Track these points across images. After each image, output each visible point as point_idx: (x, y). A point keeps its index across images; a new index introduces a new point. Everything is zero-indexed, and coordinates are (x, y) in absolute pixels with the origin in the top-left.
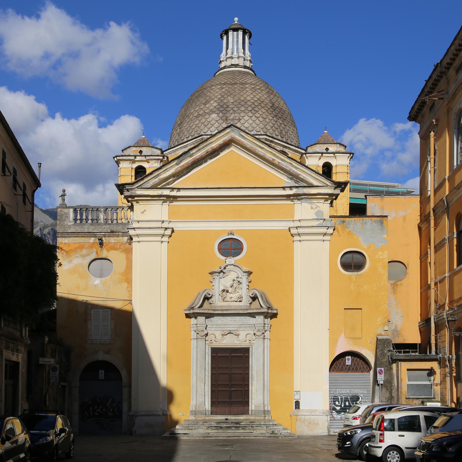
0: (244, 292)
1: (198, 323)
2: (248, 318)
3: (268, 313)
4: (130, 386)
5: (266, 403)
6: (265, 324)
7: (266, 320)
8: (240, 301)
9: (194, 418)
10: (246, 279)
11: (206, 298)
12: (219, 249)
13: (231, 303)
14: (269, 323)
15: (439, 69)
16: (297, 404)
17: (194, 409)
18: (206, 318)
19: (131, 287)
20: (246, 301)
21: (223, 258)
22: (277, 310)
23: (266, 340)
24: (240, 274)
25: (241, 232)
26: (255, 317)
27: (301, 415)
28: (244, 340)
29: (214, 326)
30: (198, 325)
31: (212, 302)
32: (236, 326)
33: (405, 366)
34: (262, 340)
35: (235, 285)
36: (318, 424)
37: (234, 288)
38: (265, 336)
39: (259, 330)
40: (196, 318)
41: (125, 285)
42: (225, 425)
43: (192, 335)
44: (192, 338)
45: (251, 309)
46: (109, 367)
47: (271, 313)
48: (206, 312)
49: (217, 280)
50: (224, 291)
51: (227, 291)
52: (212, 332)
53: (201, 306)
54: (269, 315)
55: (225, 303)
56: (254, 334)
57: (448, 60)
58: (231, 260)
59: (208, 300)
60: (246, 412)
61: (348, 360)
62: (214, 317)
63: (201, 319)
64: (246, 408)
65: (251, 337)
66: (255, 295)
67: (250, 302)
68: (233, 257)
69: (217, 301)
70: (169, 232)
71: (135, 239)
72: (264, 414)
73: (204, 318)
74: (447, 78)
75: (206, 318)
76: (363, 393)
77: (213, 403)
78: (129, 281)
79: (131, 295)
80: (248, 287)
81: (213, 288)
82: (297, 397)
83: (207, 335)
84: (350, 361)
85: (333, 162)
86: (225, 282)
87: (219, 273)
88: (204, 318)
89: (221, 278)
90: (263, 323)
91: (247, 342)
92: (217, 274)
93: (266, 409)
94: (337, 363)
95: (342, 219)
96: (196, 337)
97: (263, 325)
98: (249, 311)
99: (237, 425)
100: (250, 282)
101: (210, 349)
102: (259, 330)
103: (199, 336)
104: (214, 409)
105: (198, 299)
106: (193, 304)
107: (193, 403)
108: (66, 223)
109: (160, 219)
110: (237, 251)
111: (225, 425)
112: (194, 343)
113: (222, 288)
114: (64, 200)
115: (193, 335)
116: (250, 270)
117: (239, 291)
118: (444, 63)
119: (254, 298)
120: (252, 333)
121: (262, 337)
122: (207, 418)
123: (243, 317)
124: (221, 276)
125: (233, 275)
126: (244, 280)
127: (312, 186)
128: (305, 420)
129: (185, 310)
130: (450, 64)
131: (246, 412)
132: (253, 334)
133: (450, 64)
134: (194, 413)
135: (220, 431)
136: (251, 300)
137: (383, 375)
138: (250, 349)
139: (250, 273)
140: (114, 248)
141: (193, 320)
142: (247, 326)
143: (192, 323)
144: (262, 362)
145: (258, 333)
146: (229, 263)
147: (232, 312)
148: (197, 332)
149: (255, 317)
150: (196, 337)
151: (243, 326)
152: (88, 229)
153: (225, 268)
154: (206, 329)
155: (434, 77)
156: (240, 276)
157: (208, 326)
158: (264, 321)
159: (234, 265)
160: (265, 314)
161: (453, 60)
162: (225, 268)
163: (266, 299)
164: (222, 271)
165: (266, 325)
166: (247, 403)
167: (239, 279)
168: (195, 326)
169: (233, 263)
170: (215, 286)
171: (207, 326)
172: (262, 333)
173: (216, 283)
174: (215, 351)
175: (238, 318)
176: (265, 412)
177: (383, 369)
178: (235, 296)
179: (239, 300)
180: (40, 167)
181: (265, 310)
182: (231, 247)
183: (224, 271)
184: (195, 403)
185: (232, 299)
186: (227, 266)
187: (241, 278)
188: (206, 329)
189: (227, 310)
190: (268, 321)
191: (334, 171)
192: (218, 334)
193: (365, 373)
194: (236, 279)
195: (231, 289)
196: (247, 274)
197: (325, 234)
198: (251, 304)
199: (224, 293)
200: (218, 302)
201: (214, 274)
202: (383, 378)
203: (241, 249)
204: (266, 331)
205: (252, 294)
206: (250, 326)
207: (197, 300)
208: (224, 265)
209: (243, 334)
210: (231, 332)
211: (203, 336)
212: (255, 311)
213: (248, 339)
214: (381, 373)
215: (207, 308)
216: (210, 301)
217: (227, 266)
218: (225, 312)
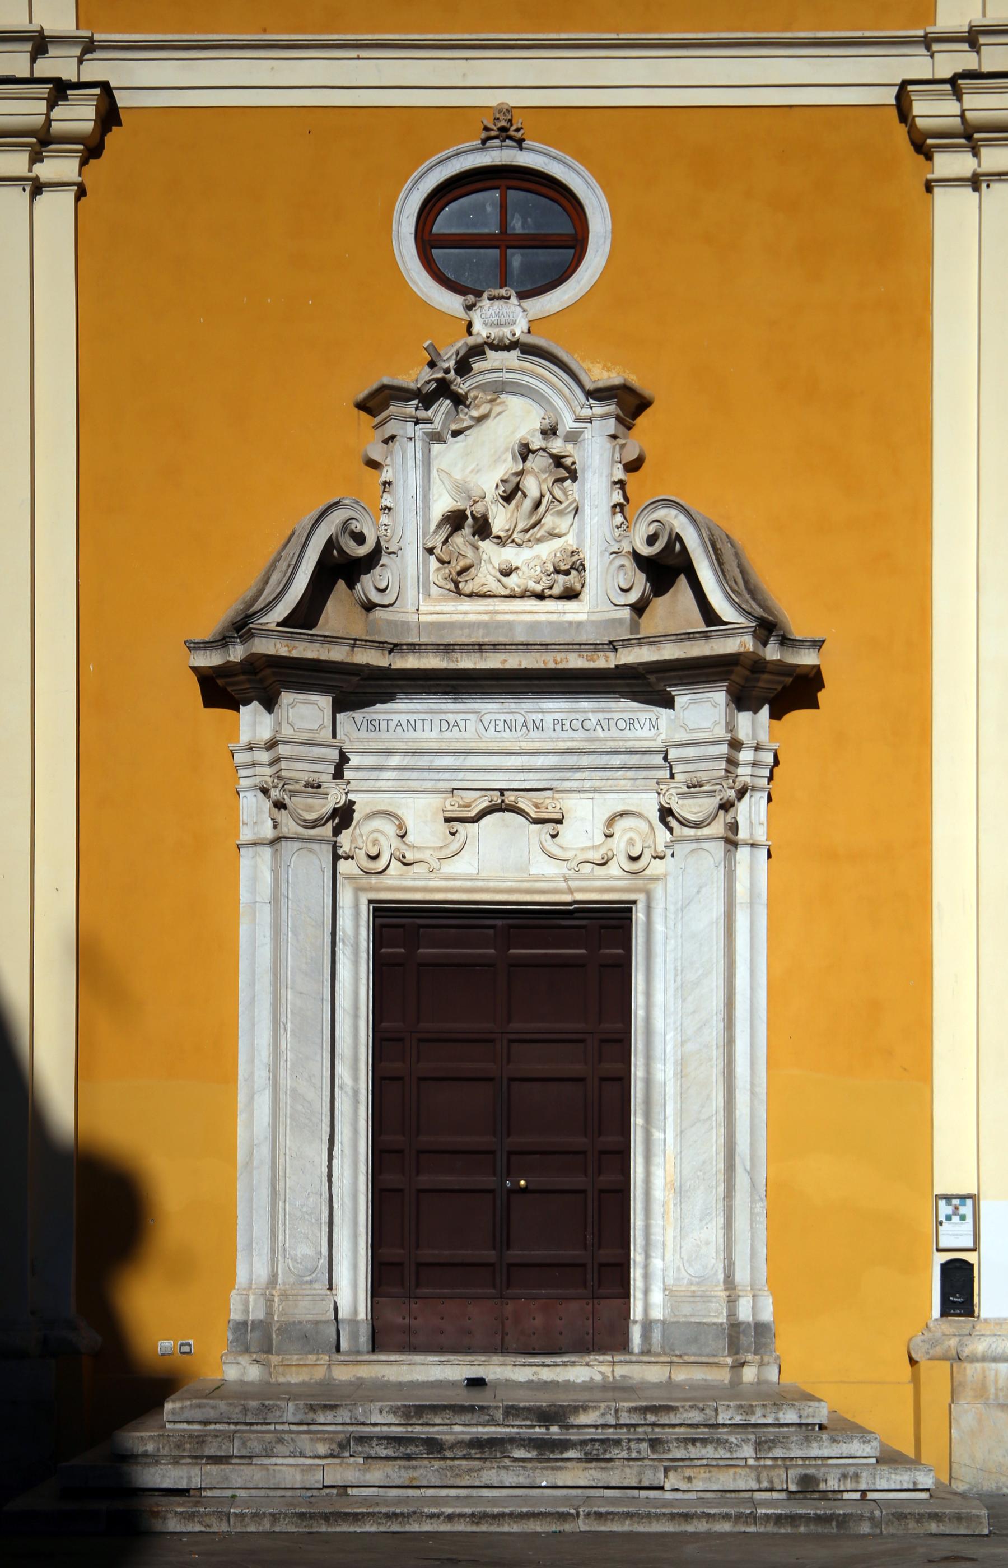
0: (594, 530)
1: (287, 732)
2: (624, 708)
3: (757, 665)
5: (742, 1275)
6: (736, 745)
7: (744, 720)
8: (571, 595)
9: (253, 1373)
10: (608, 444)
12: (427, 242)
13: (503, 607)
14: (763, 737)
17: (256, 1313)
18: (339, 706)
21: (450, 303)
22: (817, 645)
23: (743, 854)
24: (568, 407)
25: (566, 123)
26: (669, 703)
27: (984, 1359)
28: (596, 856)
29: (395, 761)
30: (282, 749)
31: (375, 597)
32: (540, 761)
34: (718, 848)
35: (531, 486)
37: (528, 504)
38: (734, 827)
39: (694, 786)
40: (270, 704)
42: (460, 1430)
43: (245, 815)
44: (246, 835)
45: (641, 642)
47: (783, 669)
48: (337, 654)
49: (413, 451)
50: (455, 520)
51: (483, 528)
52: (383, 802)
53: (305, 616)
54: (765, 681)
55: (467, 606)
56: (666, 813)
58: (503, 316)
59: (351, 586)
60: (610, 1335)
62: (388, 697)
63: (306, 711)
64: (608, 1307)
65: (642, 832)
66: (669, 546)
67: (633, 597)
68: (522, 296)
69: (411, 593)
72: (734, 1347)
73: (325, 702)
75: (339, 706)
77: (385, 1275)
80: (618, 497)
81: (387, 501)
82: (955, 1235)
83: (343, 816)
86: (473, 463)
87: (427, 400)
88: (325, 702)
89: (436, 438)
90: (720, 732)
91: (613, 869)
92: (410, 408)
93: (745, 1313)
96: (267, 831)
97: (724, 749)
98: (629, 656)
99: (549, 1428)
100: (633, 466)
101: (365, 912)
102: (694, 786)
103: (290, 826)
104: (394, 1316)
105: (282, 565)
106: (251, 606)
107: (251, 1269)
110: (543, 256)
111: (460, 1430)
112: (255, 871)
113: (443, 504)
115: (254, 815)
116: (634, 380)
117: (563, 524)
119: (664, 568)
120: (649, 805)
121: (717, 828)
122: (343, 1374)
123: (585, 704)
124: (437, 424)
125: (518, 420)
126: (596, 455)
131: (610, 1335)
132: (654, 815)
134: (257, 1337)
135: (428, 1471)
136: (640, 584)
138: (639, 916)
141: (252, 722)
142: (617, 760)
143: (244, 738)
144: (716, 1001)
145: (689, 809)
146: (495, 333)
147: (514, 661)
148: (275, 793)
149: (669, 703)
150: (267, 831)
151: (585, 760)
153: (463, 367)
154: (338, 774)
156: (568, 423)
157: (354, 760)
158: (731, 726)
159: (529, 350)
160: (740, 673)
162: (463, 367)
163: (743, 572)
164: (443, 389)
165: (745, 756)
166: (613, 1276)
167: (557, 446)
168: (264, 757)
169: (519, 329)
170: (398, 487)
171: (344, 758)
172: (714, 802)
173: (403, 465)
174: (399, 927)
175: (553, 709)
176: (743, 1339)
178: (531, 561)
183: (462, 386)
184: (262, 1272)
185: (514, 582)
186: (477, 351)
187: (573, 437)
188: (338, 774)
189: (480, 648)
190: (754, 725)
192: (422, 814)
194: (537, 442)
196: (611, 408)
198: (639, 608)
199: (459, 540)
200: (415, 600)
201: (393, 409)
203: (577, 243)
204: (742, 793)
205: (651, 540)
206: (634, 759)
207: (275, 578)
208: (462, 343)
210: (510, 798)
211: (314, 824)
212: (670, 652)
213: (619, 845)
215: (339, 635)
216: (367, 585)
217: (477, 351)
218: (467, 662)
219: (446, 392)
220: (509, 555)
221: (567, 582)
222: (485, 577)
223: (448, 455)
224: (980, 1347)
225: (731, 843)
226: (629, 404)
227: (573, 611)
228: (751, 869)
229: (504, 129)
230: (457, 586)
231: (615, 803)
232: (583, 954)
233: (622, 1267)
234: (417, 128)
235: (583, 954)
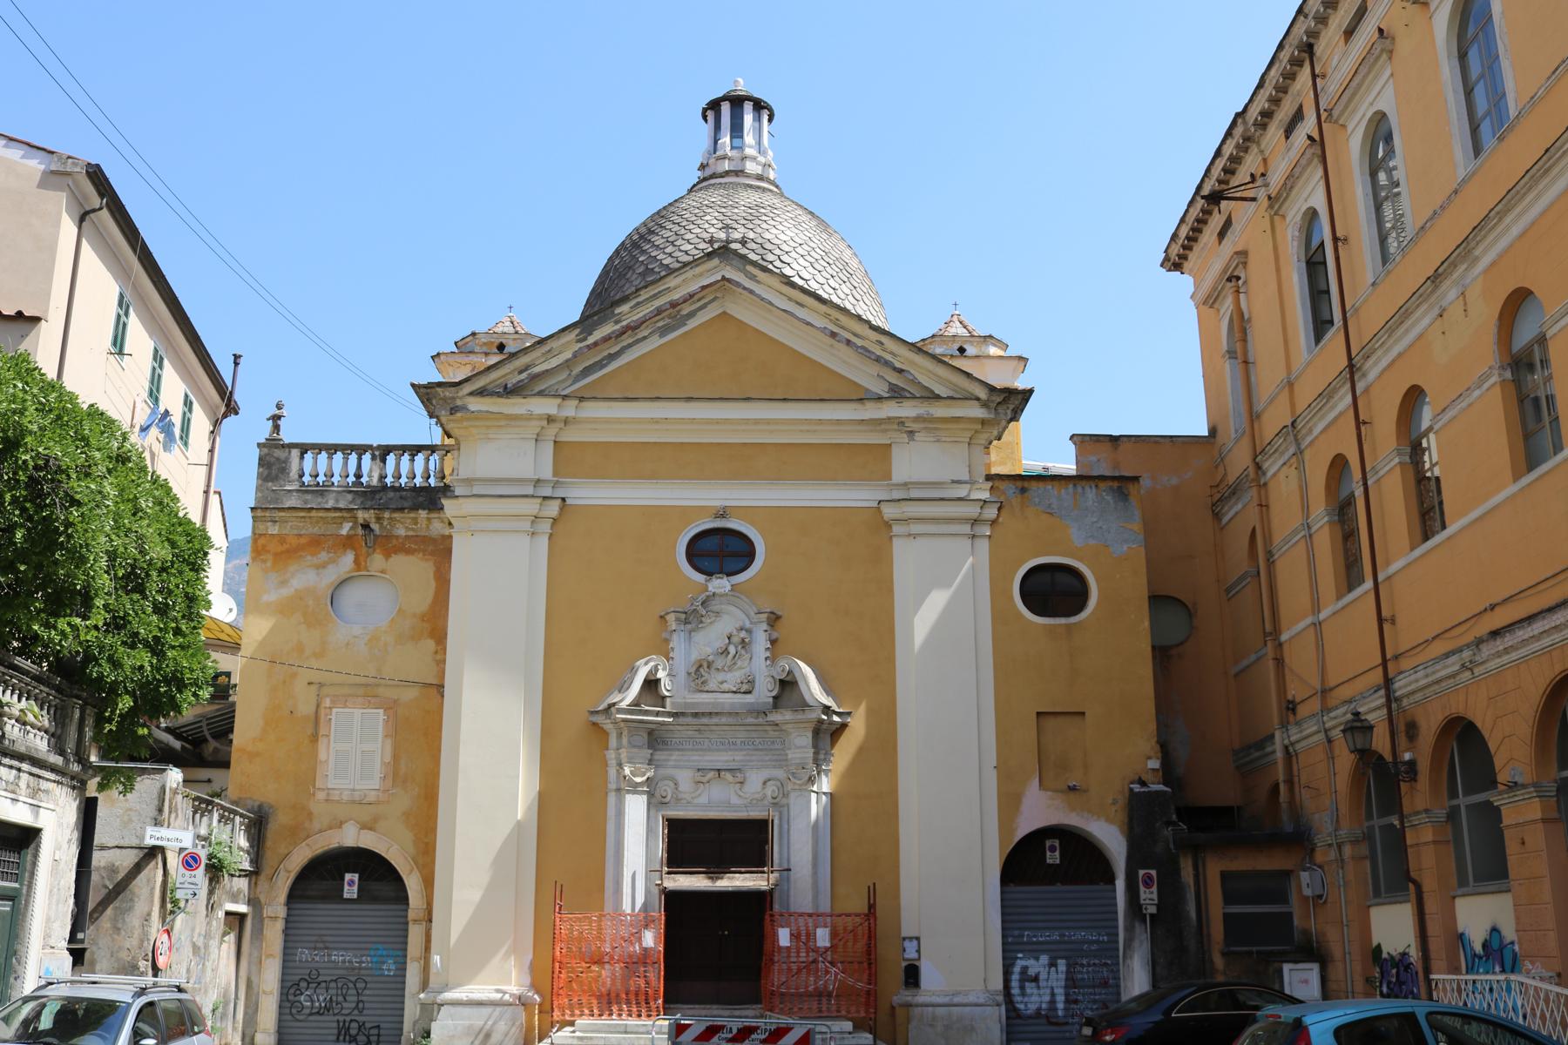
15: (1239, 131)
16: (912, 975)
19: (445, 650)
21: (700, 578)
35: (732, 650)
36: (973, 1029)
41: (430, 644)
46: (377, 873)
55: (705, 695)
57: (1261, 103)
61: (1053, 849)
68: (729, 574)
70: (553, 509)
74: (1262, 152)
76: (1097, 942)
78: (439, 636)
79: (442, 674)
84: (1057, 854)
86: (710, 638)
95: (1019, 484)
113: (695, 656)
114: (277, 428)
118: (1253, 113)
128: (934, 1018)
129: (592, 713)
130: (1267, 115)
133: (1267, 115)
137: (1155, 889)
152: (337, 501)
155: (1229, 149)
161: (1275, 101)
177: (1153, 873)
178: (733, 679)
179: (745, 687)
180: (236, 364)
185: (725, 687)
193: (1102, 886)
202: (1155, 896)
209: (755, 780)
214: (1148, 882)
220: (721, 676)
221: (748, 687)
222: (712, 685)
223: (699, 637)
224: (920, 999)
227: (749, 698)
229: (722, 514)
231: (766, 773)
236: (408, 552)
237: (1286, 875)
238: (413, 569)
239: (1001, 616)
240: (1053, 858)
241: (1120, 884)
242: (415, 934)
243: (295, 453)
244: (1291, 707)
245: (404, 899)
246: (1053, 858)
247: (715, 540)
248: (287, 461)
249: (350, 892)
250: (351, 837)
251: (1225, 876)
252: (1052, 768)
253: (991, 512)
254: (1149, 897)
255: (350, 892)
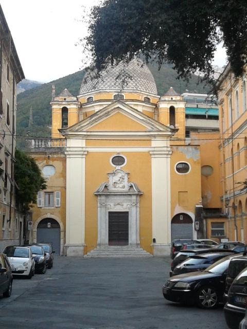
0: (126, 183)
4: (65, 232)
11: (106, 187)
13: (119, 189)
16: (154, 240)
20: (126, 189)
33: (210, 221)
41: (62, 179)
46: (54, 222)
50: (115, 183)
58: (118, 167)
63: (103, 198)
71: (67, 156)
77: (110, 240)
78: (64, 177)
79: (66, 184)
85: (176, 106)
86: (116, 178)
94: (176, 219)
107: (99, 240)
108: (30, 147)
109: (81, 146)
113: (114, 181)
115: (99, 205)
125: (120, 175)
126: (126, 177)
127: (161, 131)
139: (128, 174)
140: (54, 160)
141: (99, 198)
164: (114, 173)
166: (127, 240)
173: (111, 179)
178: (121, 185)
181: (137, 193)
182: (118, 160)
191: (176, 111)
192: (112, 205)
195: (119, 181)
197: (167, 154)
200: (112, 189)
209: (125, 205)
214: (197, 224)
219: (114, 174)
221: (124, 187)
223: (114, 177)
225: (136, 207)
226: (128, 174)
228: (138, 209)
230: (115, 187)
232: (124, 216)
233: (128, 240)
234: (111, 153)
235: (124, 216)
236: (57, 160)
237: (223, 223)
238: (58, 164)
239: (172, 173)
240: (181, 219)
241: (193, 224)
242: (62, 234)
243: (33, 140)
244: (226, 192)
245: (60, 228)
246: (181, 219)
247: (117, 158)
248: (32, 142)
249: (49, 226)
250: (49, 216)
251: (212, 223)
252: (181, 202)
253: (171, 153)
254: (198, 227)
255: (49, 226)
